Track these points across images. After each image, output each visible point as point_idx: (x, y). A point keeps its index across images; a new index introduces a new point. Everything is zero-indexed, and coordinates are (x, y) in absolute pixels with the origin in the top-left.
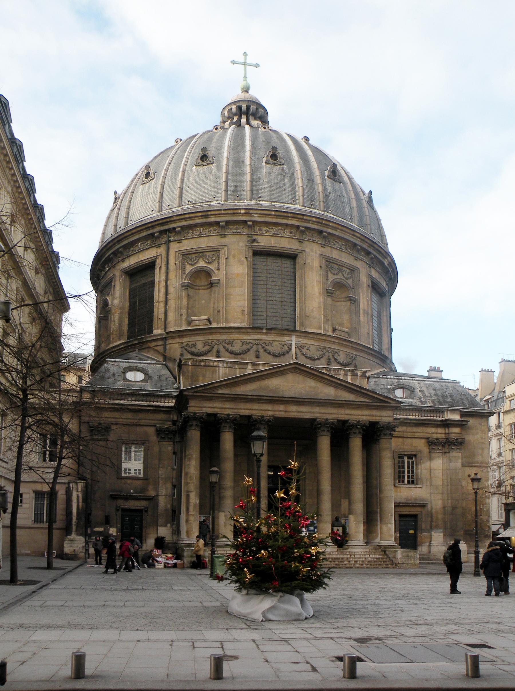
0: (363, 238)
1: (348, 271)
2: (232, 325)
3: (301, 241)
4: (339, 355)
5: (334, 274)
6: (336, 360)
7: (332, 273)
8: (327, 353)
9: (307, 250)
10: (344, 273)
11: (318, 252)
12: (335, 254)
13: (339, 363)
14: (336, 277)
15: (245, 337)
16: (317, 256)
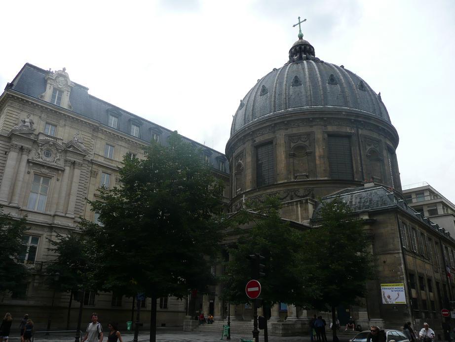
0: (312, 113)
1: (306, 136)
2: (247, 190)
3: (274, 132)
4: (299, 192)
5: (295, 143)
6: (296, 195)
7: (293, 142)
8: (290, 193)
9: (277, 135)
10: (302, 139)
11: (284, 134)
12: (295, 131)
13: (299, 196)
14: (295, 144)
15: (252, 195)
16: (283, 136)
